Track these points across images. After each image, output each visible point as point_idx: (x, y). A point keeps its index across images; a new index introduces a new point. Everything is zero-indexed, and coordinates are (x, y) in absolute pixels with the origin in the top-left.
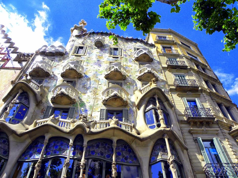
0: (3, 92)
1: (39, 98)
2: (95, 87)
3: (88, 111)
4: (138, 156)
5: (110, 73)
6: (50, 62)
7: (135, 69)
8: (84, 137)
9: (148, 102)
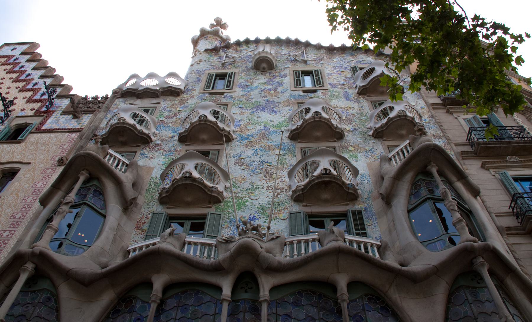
0: (40, 184)
1: (130, 193)
2: (267, 162)
3: (258, 219)
5: (303, 124)
6: (150, 111)
7: (362, 113)
8: (258, 276)
9: (412, 185)
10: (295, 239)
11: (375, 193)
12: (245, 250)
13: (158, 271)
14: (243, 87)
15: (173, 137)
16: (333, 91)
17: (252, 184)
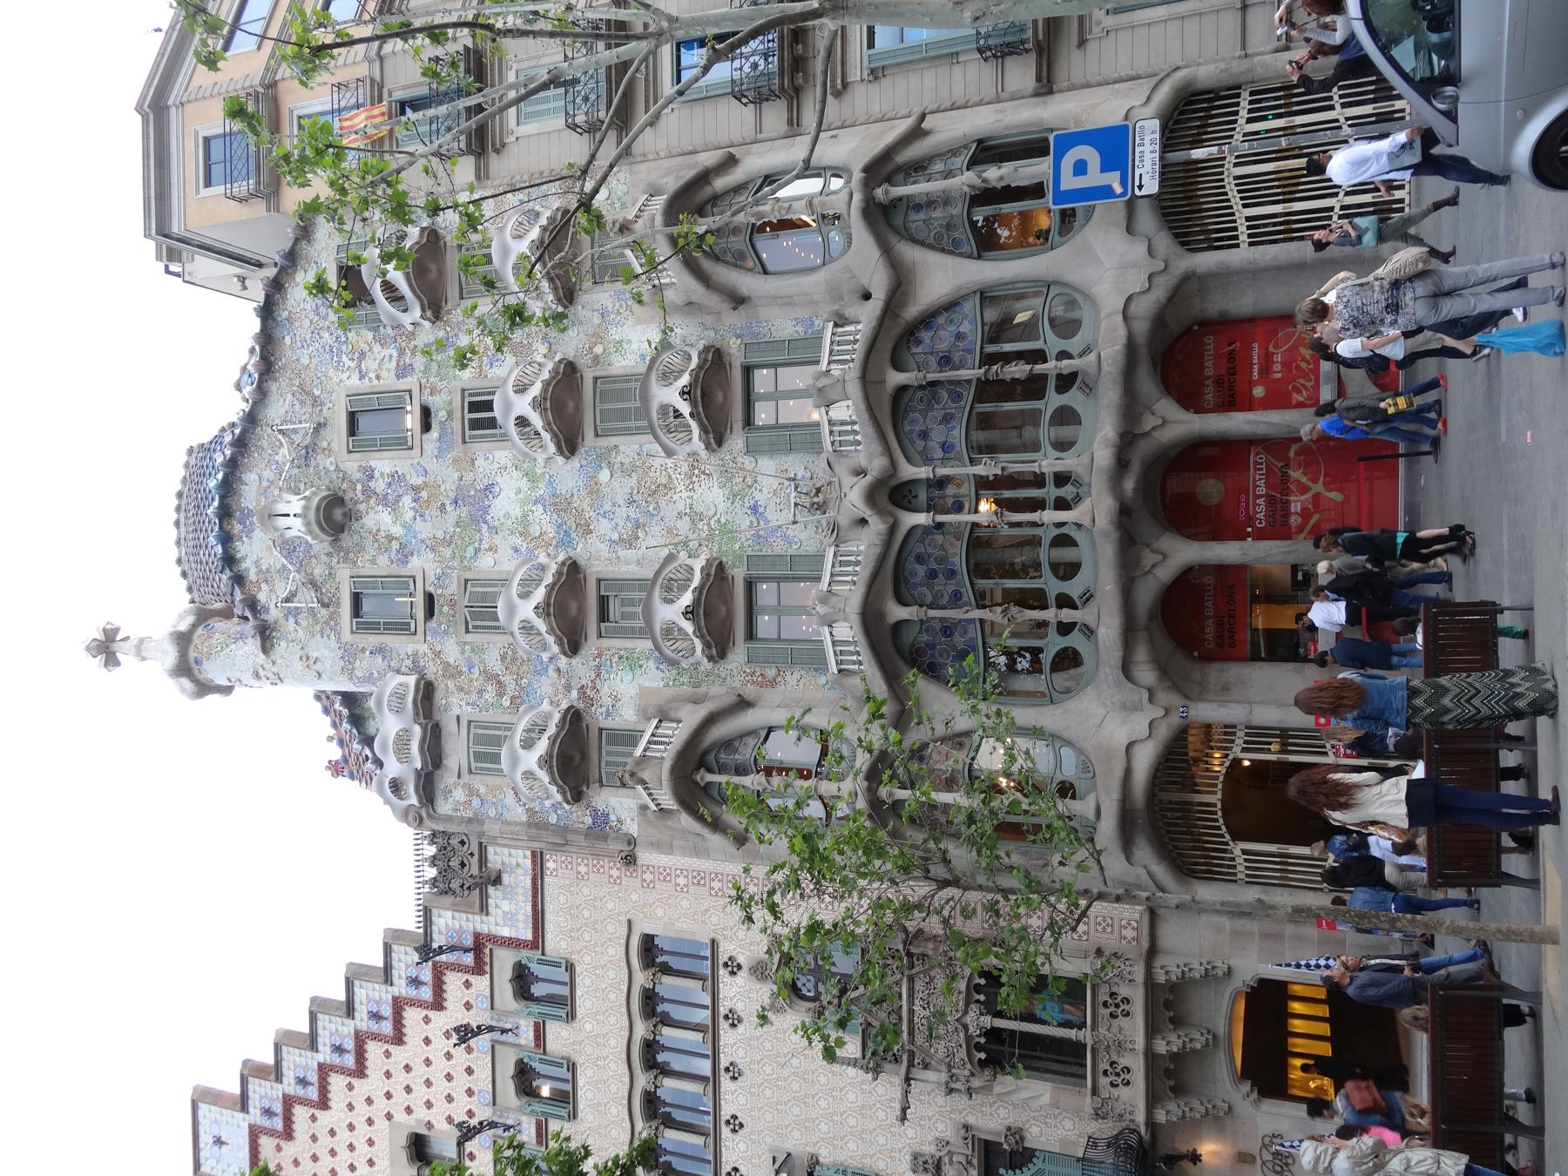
4: (950, 298)
10: (827, 440)
11: (709, 319)
12: (871, 497)
13: (881, 615)
14: (405, 554)
15: (558, 670)
16: (425, 372)
17: (680, 515)
